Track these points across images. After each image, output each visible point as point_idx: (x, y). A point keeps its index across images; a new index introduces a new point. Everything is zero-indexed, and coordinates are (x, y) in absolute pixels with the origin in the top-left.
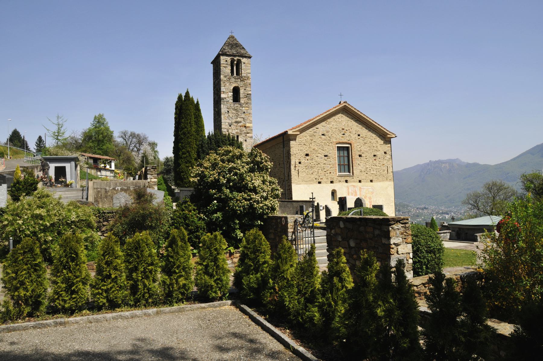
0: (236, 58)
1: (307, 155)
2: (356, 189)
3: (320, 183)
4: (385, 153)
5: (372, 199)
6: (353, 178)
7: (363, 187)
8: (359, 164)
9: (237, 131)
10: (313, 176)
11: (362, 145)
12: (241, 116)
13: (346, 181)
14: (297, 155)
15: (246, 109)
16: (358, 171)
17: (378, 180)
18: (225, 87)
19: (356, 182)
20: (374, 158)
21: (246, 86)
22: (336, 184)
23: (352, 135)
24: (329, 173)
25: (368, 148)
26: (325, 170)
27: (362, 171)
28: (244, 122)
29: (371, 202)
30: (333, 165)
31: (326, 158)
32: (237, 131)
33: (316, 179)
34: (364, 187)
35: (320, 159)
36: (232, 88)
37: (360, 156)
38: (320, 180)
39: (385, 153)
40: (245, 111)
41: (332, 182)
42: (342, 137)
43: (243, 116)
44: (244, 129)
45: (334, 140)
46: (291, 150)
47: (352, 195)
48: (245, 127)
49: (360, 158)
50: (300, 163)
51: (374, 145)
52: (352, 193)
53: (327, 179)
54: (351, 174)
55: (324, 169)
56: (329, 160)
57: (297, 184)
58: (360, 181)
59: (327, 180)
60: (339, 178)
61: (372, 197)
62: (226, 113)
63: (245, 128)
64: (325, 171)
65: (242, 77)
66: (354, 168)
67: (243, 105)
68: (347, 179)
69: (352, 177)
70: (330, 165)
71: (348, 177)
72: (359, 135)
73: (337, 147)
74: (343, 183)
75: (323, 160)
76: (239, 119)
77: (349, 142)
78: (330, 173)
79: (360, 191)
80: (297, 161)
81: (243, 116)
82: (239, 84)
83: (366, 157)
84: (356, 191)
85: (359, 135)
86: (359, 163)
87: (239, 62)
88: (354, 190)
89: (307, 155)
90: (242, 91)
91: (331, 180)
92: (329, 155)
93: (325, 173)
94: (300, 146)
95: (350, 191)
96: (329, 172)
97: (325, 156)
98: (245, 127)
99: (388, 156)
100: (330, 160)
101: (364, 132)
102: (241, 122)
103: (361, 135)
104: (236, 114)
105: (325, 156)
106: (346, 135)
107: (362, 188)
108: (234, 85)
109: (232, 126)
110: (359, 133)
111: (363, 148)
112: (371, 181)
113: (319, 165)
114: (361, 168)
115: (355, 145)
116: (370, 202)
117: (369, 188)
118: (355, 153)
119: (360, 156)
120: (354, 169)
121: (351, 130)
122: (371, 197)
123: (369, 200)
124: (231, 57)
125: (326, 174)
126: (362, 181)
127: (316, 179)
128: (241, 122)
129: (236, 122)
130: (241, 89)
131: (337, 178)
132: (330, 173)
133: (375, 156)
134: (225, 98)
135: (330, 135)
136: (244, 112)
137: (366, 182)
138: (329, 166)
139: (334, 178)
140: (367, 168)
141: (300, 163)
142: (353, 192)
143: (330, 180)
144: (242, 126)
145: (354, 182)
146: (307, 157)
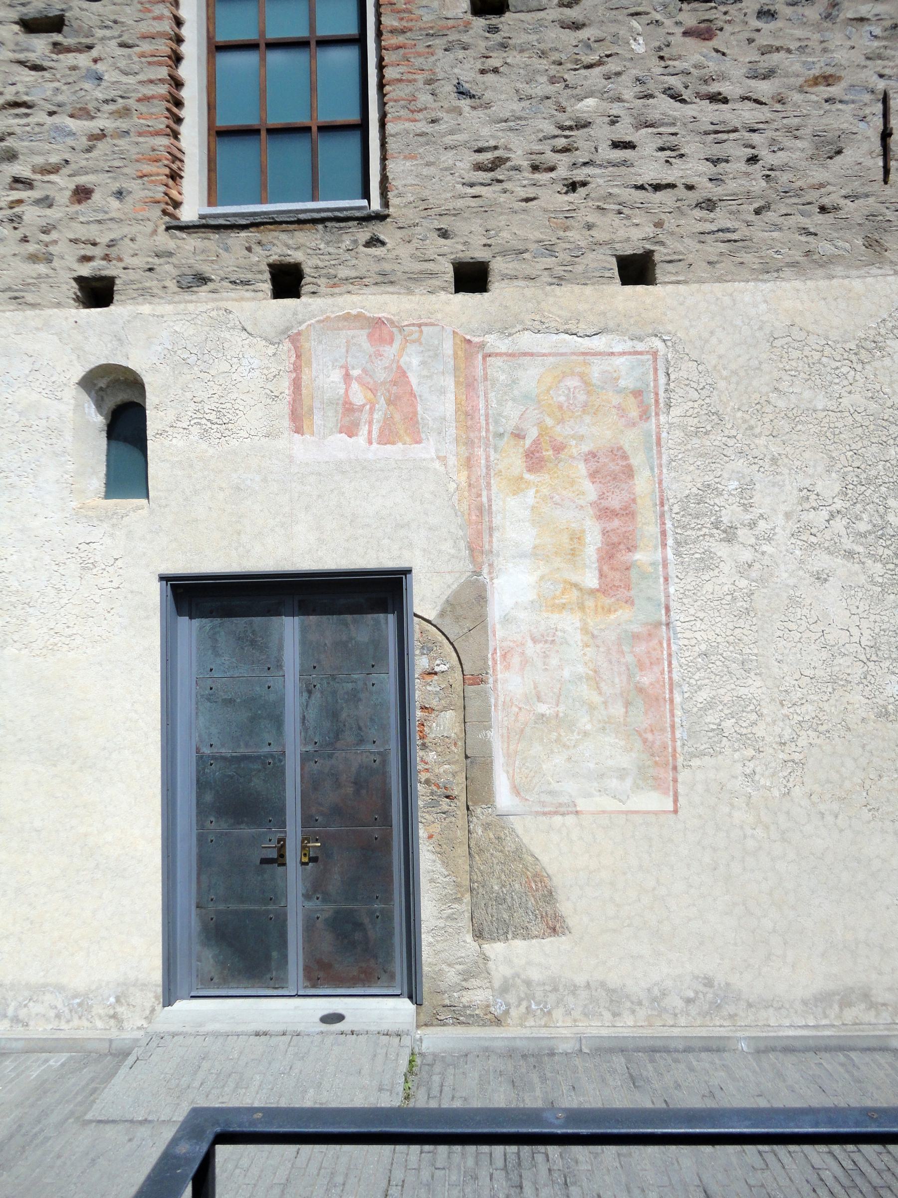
2: (412, 360)
5: (642, 484)
6: (375, 242)
7: (505, 331)
8: (462, 93)
16: (448, 158)
19: (416, 278)
22: (146, 309)
24: (64, 198)
26: (21, 169)
27: (496, 164)
29: (628, 512)
30: (125, 112)
31: (40, 44)
34: (527, 341)
47: (351, 431)
52: (349, 408)
53: (33, 258)
54: (376, 205)
56: (69, 59)
59: (42, 268)
60: (191, 242)
61: (637, 460)
64: (18, 181)
66: (390, 128)
68: (297, 256)
69: (364, 234)
70: (82, 113)
74: (242, 292)
78: (82, 194)
84: (401, 375)
86: (467, 74)
88: (381, 376)
91: (85, 271)
93: (16, 195)
96: (64, 183)
100: (83, 60)
107: (494, 342)
114: (488, 134)
116: (604, 513)
117: (598, 343)
120: (392, 145)
122: (618, 453)
123: (591, 490)
126: (498, 266)
131: (165, 241)
132: (82, 194)
137: (560, 280)
138: (73, 124)
139: (125, 248)
140: (587, 125)
142: (358, 396)
145: (385, 279)
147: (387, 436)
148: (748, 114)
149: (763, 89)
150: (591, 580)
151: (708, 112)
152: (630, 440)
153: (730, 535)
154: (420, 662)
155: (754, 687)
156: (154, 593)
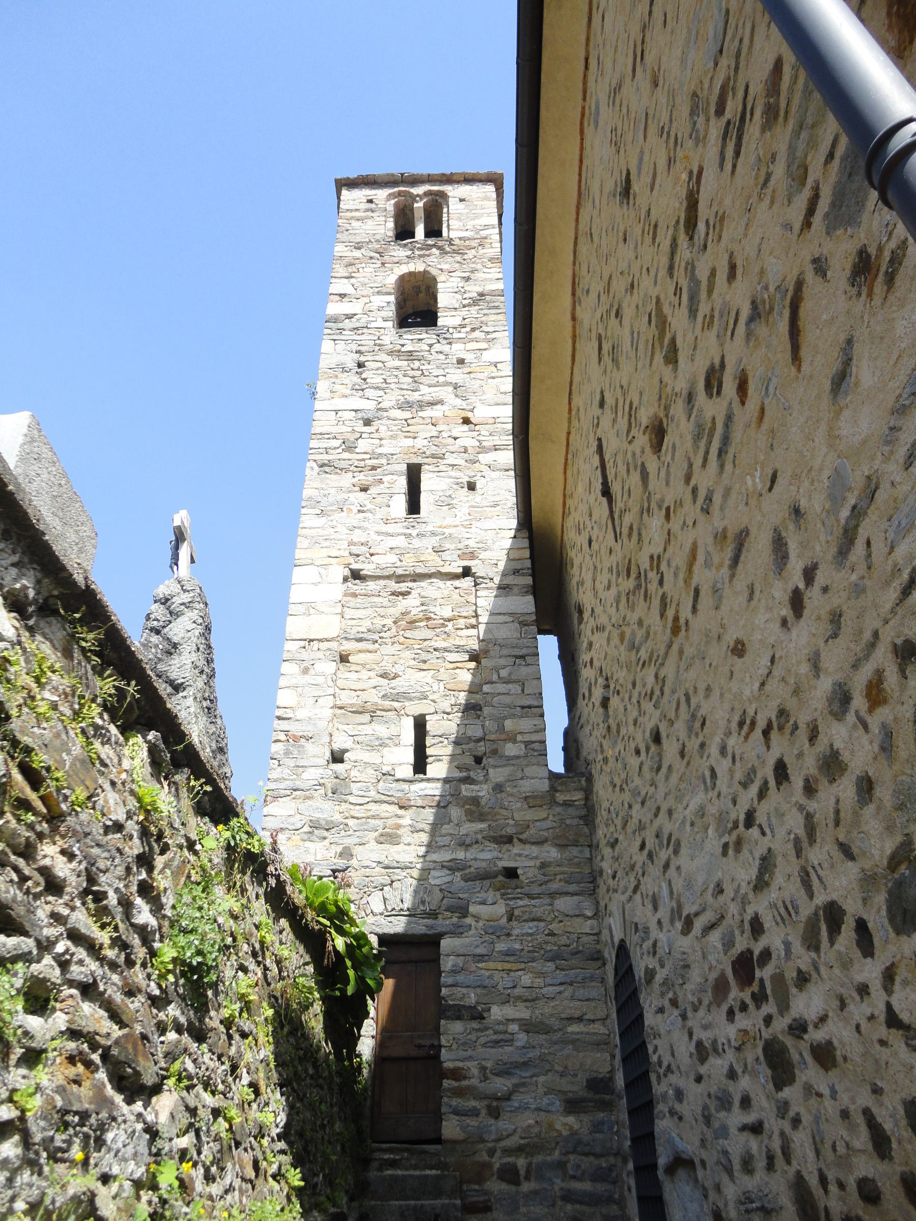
0: (419, 190)
12: (442, 379)
18: (353, 280)
28: (458, 402)
36: (391, 280)
40: (469, 357)
43: (456, 376)
62: (344, 370)
63: (466, 427)
65: (450, 241)
67: (456, 335)
76: (426, 392)
81: (456, 376)
98: (466, 421)
104: (411, 373)
109: (382, 426)
124: (396, 189)
129: (406, 405)
136: (461, 362)
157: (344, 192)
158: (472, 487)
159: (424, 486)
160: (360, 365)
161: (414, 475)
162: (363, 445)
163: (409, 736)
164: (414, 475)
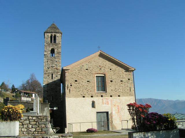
1: (76, 81)
3: (84, 97)
4: (129, 79)
9: (52, 71)
10: (79, 93)
11: (112, 75)
13: (102, 96)
14: (69, 81)
15: (58, 59)
17: (124, 96)
20: (121, 82)
21: (58, 48)
23: (106, 69)
25: (117, 77)
29: (119, 108)
31: (88, 82)
32: (52, 71)
33: (81, 95)
34: (114, 100)
35: (85, 83)
36: (50, 49)
37: (111, 81)
38: (84, 95)
39: (129, 79)
40: (57, 61)
41: (92, 97)
42: (99, 71)
44: (56, 70)
45: (94, 72)
46: (66, 78)
47: (105, 104)
48: (57, 69)
49: (111, 82)
50: (71, 85)
51: (121, 75)
55: (87, 89)
57: (69, 97)
58: (111, 96)
71: (103, 94)
72: (111, 69)
73: (96, 76)
75: (87, 83)
76: (54, 65)
77: (104, 73)
78: (91, 91)
79: (111, 102)
80: (69, 85)
82: (54, 47)
83: (115, 82)
84: (108, 102)
85: (111, 69)
87: (55, 37)
89: (76, 81)
90: (56, 51)
91: (91, 95)
92: (90, 81)
94: (71, 76)
95: (104, 101)
97: (87, 81)
99: (131, 81)
100: (91, 84)
101: (114, 67)
102: (54, 67)
103: (112, 69)
105: (87, 81)
106: (102, 69)
108: (52, 48)
109: (50, 69)
110: (110, 68)
111: (113, 77)
112: (119, 96)
113: (84, 87)
114: (112, 89)
115: (108, 75)
118: (108, 80)
119: (111, 81)
121: (105, 66)
125: (88, 92)
127: (81, 95)
128: (54, 67)
130: (55, 49)
132: (91, 91)
133: (121, 81)
134: (46, 54)
135: (91, 70)
141: (71, 85)
143: (90, 95)
144: (55, 69)
146: (76, 82)
147: (107, 104)
148: (124, 88)
149: (125, 86)
150: (117, 112)
151: (122, 88)
152: (119, 105)
153: (124, 110)
154: (109, 116)
155: (125, 117)
156: (96, 113)
157: (45, 34)
158: (57, 76)
159: (53, 76)
160: (48, 61)
161: (52, 74)
162: (48, 71)
163: (52, 98)
164: (52, 74)
